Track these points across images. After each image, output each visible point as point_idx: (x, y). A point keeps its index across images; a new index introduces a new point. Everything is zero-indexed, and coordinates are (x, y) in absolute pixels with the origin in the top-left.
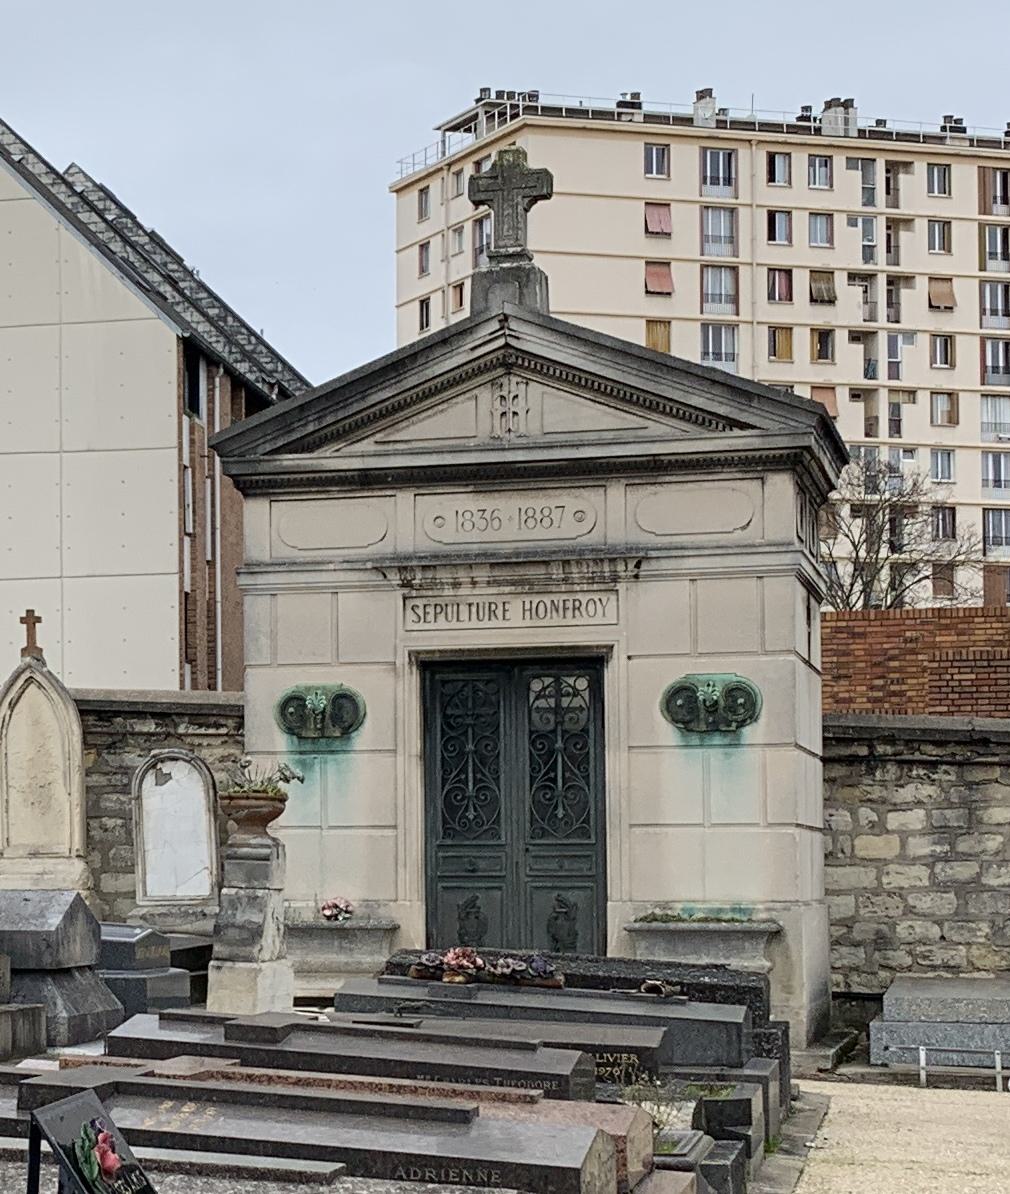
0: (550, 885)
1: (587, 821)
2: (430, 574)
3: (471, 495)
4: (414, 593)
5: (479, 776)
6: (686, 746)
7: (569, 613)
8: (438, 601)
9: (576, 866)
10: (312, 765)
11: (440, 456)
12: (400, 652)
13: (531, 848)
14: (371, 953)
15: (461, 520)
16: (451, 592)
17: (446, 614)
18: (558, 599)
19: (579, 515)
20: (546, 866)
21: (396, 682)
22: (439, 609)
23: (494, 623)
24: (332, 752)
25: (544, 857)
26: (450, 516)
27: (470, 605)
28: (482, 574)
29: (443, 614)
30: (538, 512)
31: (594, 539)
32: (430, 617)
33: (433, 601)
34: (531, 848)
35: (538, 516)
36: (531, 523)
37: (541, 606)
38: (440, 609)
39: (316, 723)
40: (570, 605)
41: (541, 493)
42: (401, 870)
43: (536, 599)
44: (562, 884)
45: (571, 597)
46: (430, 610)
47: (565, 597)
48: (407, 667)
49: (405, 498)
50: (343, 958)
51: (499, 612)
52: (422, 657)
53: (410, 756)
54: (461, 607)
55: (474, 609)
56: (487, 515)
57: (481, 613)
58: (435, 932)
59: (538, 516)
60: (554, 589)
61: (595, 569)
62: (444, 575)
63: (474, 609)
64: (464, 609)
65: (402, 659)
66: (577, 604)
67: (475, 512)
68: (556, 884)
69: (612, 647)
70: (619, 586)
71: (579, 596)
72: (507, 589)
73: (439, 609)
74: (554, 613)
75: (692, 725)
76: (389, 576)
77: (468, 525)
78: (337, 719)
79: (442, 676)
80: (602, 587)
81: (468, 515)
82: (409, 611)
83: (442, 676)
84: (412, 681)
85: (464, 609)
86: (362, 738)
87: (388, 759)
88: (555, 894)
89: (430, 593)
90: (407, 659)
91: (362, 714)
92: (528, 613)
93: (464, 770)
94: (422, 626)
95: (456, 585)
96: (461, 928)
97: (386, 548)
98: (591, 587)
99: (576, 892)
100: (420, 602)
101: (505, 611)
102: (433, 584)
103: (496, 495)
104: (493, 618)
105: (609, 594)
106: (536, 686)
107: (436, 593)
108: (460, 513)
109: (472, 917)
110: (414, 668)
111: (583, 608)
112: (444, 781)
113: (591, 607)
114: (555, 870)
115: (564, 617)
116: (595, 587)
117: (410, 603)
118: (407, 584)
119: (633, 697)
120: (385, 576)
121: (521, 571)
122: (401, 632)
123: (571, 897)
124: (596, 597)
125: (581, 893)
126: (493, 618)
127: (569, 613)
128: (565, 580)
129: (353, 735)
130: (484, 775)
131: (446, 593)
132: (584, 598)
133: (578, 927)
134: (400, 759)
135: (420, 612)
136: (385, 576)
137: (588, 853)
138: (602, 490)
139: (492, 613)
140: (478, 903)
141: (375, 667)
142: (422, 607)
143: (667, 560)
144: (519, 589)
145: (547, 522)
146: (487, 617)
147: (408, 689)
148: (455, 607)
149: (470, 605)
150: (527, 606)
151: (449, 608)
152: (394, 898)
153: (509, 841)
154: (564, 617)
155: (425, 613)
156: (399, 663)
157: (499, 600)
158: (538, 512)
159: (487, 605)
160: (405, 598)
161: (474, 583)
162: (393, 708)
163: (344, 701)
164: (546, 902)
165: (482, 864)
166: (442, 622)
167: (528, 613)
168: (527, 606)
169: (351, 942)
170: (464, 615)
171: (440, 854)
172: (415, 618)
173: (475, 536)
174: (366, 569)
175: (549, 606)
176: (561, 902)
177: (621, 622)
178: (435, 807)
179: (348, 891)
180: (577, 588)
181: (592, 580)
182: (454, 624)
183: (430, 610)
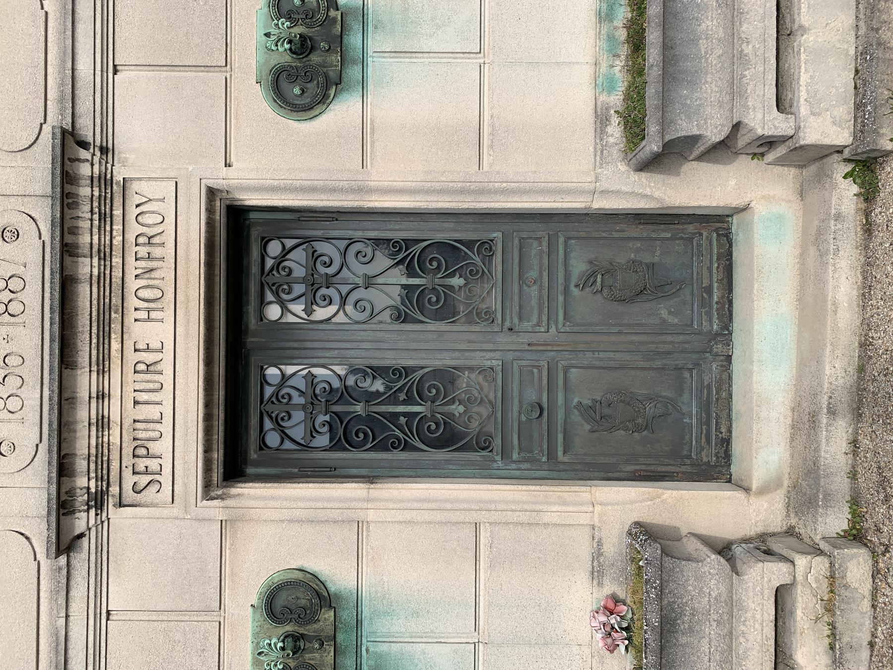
0: (561, 298)
1: (469, 244)
2: (81, 465)
4: (114, 490)
5: (402, 396)
6: (363, 83)
7: (157, 252)
8: (128, 450)
9: (535, 262)
10: (380, 656)
12: (208, 513)
13: (507, 324)
14: (699, 578)
16: (115, 431)
19: (7, 234)
20: (534, 302)
21: (258, 521)
22: (143, 451)
23: (167, 367)
24: (359, 623)
25: (520, 307)
27: (136, 403)
28: (85, 382)
29: (150, 445)
31: (44, 213)
32: (153, 464)
33: (128, 460)
34: (507, 324)
36: (15, 308)
37: (143, 294)
38: (141, 449)
39: (313, 651)
40: (143, 251)
42: (546, 518)
43: (132, 302)
44: (561, 281)
45: (131, 250)
46: (141, 464)
50: (711, 630)
51: (150, 358)
52: (217, 475)
53: (368, 500)
54: (137, 418)
55: (143, 397)
57: (151, 386)
58: (630, 468)
60: (117, 273)
61: (87, 208)
62: (83, 443)
63: (143, 397)
64: (144, 412)
65: (215, 509)
66: (141, 240)
68: (561, 288)
69: (212, 193)
70: (118, 178)
71: (131, 237)
72: (115, 345)
73: (143, 451)
74: (155, 274)
75: (332, 75)
76: (77, 532)
77: (13, 404)
78: (306, 615)
79: (238, 450)
80: (118, 202)
83: (238, 450)
84: (250, 493)
85: (144, 412)
86: (338, 574)
87: (374, 539)
88: (575, 291)
89: (115, 465)
90: (215, 503)
91: (300, 575)
93: (394, 417)
94: (166, 478)
95: (102, 423)
96: (626, 429)
97: (40, 532)
99: (573, 262)
100: (129, 480)
101: (148, 349)
104: (159, 367)
105: (130, 193)
106: (274, 312)
107: (115, 456)
109: (606, 411)
111: (150, 232)
112: (407, 447)
113: (148, 219)
114: (540, 291)
116: (118, 212)
117: (129, 495)
118: (98, 501)
119: (283, 161)
120: (81, 536)
122: (175, 511)
123: (579, 267)
124: (132, 212)
125: (573, 255)
126: (159, 367)
127: (157, 252)
128: (105, 256)
129: (332, 589)
130: (400, 390)
131: (115, 439)
132: (134, 230)
133: (622, 259)
134: (371, 515)
135: (144, 480)
136: (81, 536)
137: (516, 241)
140: (587, 402)
141: (227, 553)
142: (136, 478)
143: (78, 102)
144: (116, 327)
145: (15, 284)
146: (156, 377)
147: (262, 500)
149: (136, 403)
150: (143, 315)
151: (141, 435)
152: (588, 530)
153: (498, 355)
155: (147, 472)
156: (220, 515)
157: (131, 357)
160: (121, 505)
161: (102, 396)
162: (291, 525)
163: (278, 609)
164: (587, 305)
165: (531, 395)
166: (162, 447)
167: (153, 315)
168: (143, 315)
169: (682, 614)
170: (152, 412)
171: (515, 456)
172: (154, 488)
173: (31, 395)
174: (68, 565)
175: (141, 282)
176: (587, 282)
177: (172, 175)
178: (448, 462)
179: (578, 604)
180: (118, 240)
183: (141, 464)
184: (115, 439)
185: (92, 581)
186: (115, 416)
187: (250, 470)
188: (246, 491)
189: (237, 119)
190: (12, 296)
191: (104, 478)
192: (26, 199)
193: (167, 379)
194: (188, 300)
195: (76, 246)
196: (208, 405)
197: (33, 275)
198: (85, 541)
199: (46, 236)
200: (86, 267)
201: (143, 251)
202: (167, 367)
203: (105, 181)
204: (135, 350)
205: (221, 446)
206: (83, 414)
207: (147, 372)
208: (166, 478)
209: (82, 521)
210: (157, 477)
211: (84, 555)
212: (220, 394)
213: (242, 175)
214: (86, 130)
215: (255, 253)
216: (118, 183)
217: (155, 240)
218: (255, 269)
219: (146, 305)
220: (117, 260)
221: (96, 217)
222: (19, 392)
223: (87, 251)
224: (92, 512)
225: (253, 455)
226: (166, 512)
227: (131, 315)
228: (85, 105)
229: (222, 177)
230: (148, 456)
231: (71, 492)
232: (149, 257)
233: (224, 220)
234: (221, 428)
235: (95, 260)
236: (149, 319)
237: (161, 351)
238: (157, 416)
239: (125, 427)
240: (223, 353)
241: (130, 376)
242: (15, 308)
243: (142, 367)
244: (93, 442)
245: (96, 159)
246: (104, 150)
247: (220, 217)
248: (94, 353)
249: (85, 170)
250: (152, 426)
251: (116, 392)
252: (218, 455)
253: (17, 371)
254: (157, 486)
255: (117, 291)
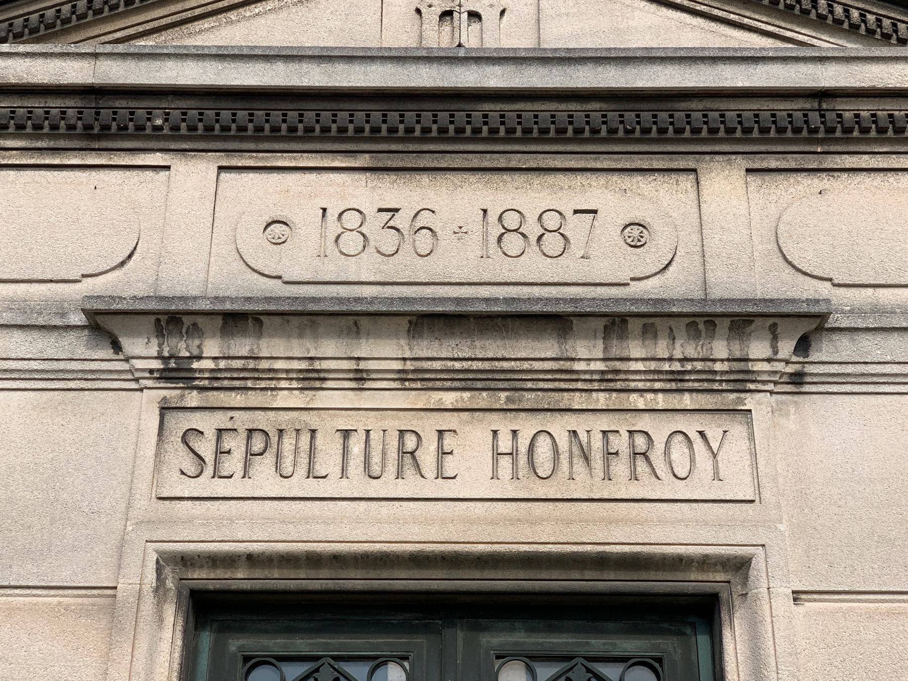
2: (242, 346)
3: (362, 177)
4: (193, 399)
7: (620, 468)
8: (261, 420)
11: (294, 66)
15: (333, 228)
16: (296, 400)
17: (278, 456)
18: (591, 428)
19: (636, 231)
21: (107, 658)
22: (258, 444)
23: (410, 486)
26: (305, 216)
27: (346, 434)
28: (385, 351)
30: (531, 218)
31: (677, 285)
33: (243, 420)
35: (532, 229)
36: (513, 243)
37: (543, 444)
38: (262, 442)
40: (620, 443)
41: (536, 180)
43: (528, 427)
45: (623, 424)
46: (236, 444)
47: (604, 422)
48: (149, 602)
49: (192, 176)
51: (428, 457)
52: (204, 578)
54: (319, 435)
56: (402, 221)
57: (376, 459)
59: (532, 229)
60: (578, 400)
61: (691, 352)
62: (279, 350)
63: (356, 446)
65: (138, 574)
66: (640, 441)
67: (370, 210)
69: (740, 566)
70: (750, 402)
71: (644, 423)
72: (449, 399)
74: (579, 466)
76: (125, 342)
77: (352, 242)
81: (352, 219)
82: (175, 439)
89: (237, 399)
90: (151, 577)
92: (505, 462)
94: (206, 485)
95: (312, 378)
97: (131, 285)
98: (674, 401)
100: (208, 423)
101: (443, 453)
102: (252, 376)
103: (425, 179)
104: (409, 472)
107: (253, 399)
108: (332, 214)
110: (170, 611)
111: (657, 456)
113: (679, 452)
115: (608, 477)
116: (687, 401)
117: (180, 423)
118: (175, 373)
120: (117, 347)
121: (491, 348)
122: (143, 503)
124: (691, 425)
126: (409, 472)
127: (620, 468)
128: (609, 380)
131: (283, 399)
135: (206, 449)
136: (117, 347)
138: (687, 182)
139: (409, 457)
142: (210, 434)
143: (879, 338)
144: (483, 399)
145: (553, 243)
146: (392, 468)
148: (305, 438)
149: (346, 434)
150: (505, 444)
151: (288, 443)
154: (608, 477)
155: (221, 452)
156: (126, 586)
157: (428, 426)
158: (531, 218)
159: (393, 442)
160: (165, 409)
161: (360, 378)
166: (263, 477)
167: (505, 462)
168: (505, 444)
172: (190, 466)
173: (366, 268)
174: (68, 328)
175: (563, 441)
177: (767, 494)
180: (639, 401)
181: (677, 381)
182: (299, 485)
183: (236, 444)
184: (283, 399)
185: (34, 365)
186: (323, 399)
187: (206, 639)
188: (167, 634)
189: (889, 613)
190: (533, 239)
191: (215, 381)
192: (697, 258)
193: (388, 486)
194: (533, 523)
195: (623, 335)
196: (338, 560)
197: (570, 268)
198: (108, 353)
199: (636, 289)
200: (588, 353)
201: (620, 443)
202: (410, 486)
203: (742, 380)
204: (441, 432)
205: (258, 585)
206: (330, 350)
207: (402, 452)
208: (206, 485)
209: (143, 350)
210: (209, 470)
211: (82, 351)
212: (357, 581)
213: (780, 624)
214: (828, 352)
215: (630, 645)
216: (741, 401)
217: (641, 464)
218: (597, 644)
219: (523, 448)
220: (601, 400)
221: (677, 366)
222: (370, 250)
223: (615, 352)
224: (156, 365)
225: (236, 644)
226: (143, 486)
227: (504, 424)
228: (874, 348)
229: (773, 583)
230: (249, 455)
231: (195, 331)
232: (610, 455)
233: (690, 587)
234: (292, 585)
235: (600, 366)
236: (497, 454)
237: (440, 475)
238: (320, 470)
239: (305, 416)
240: (434, 585)
241: (394, 423)
242: (513, 243)
243: (410, 442)
244: (279, 365)
245: (780, 367)
246: (797, 379)
247: (695, 582)
248: (437, 365)
249: (758, 349)
250: (304, 460)
251: (367, 400)
252: (241, 579)
253: (407, 247)
254: (192, 470)
255: (545, 401)
